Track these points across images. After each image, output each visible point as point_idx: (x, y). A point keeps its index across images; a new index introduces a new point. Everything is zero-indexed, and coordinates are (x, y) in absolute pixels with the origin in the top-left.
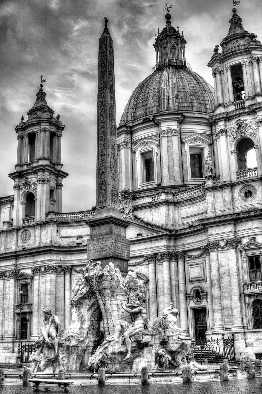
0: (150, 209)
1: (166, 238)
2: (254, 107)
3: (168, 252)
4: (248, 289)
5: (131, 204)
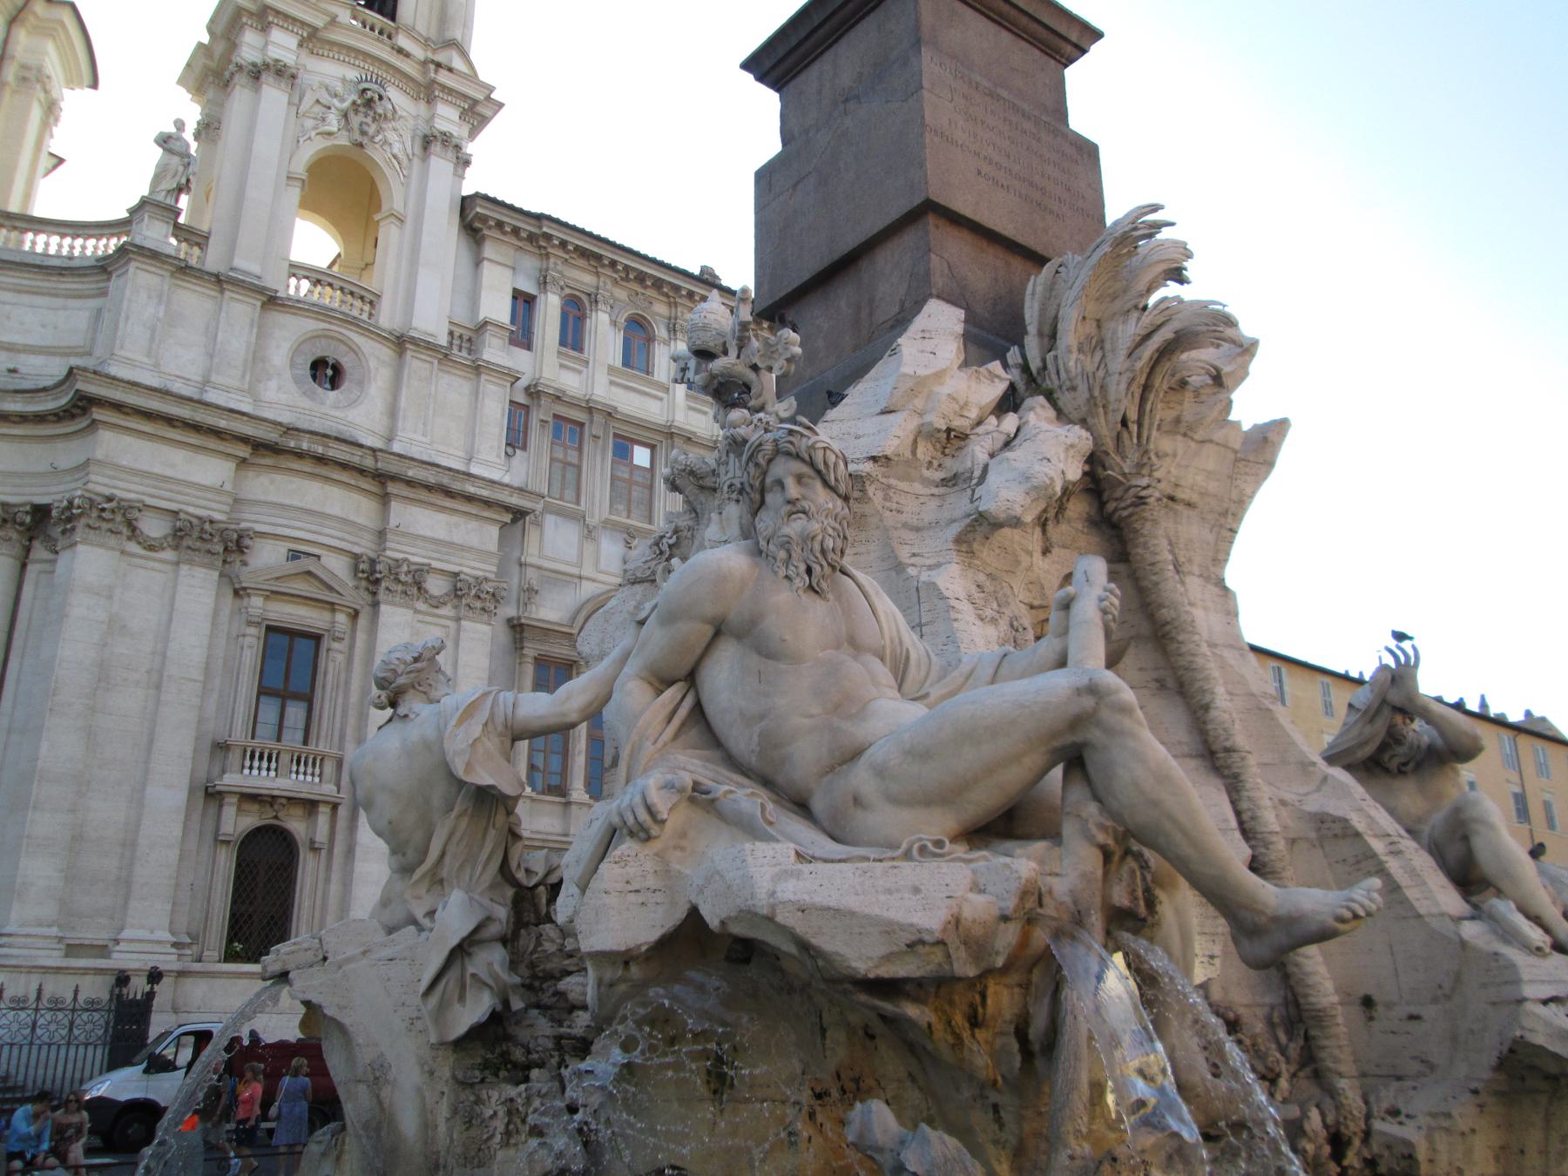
2: (443, 77)
4: (246, 771)
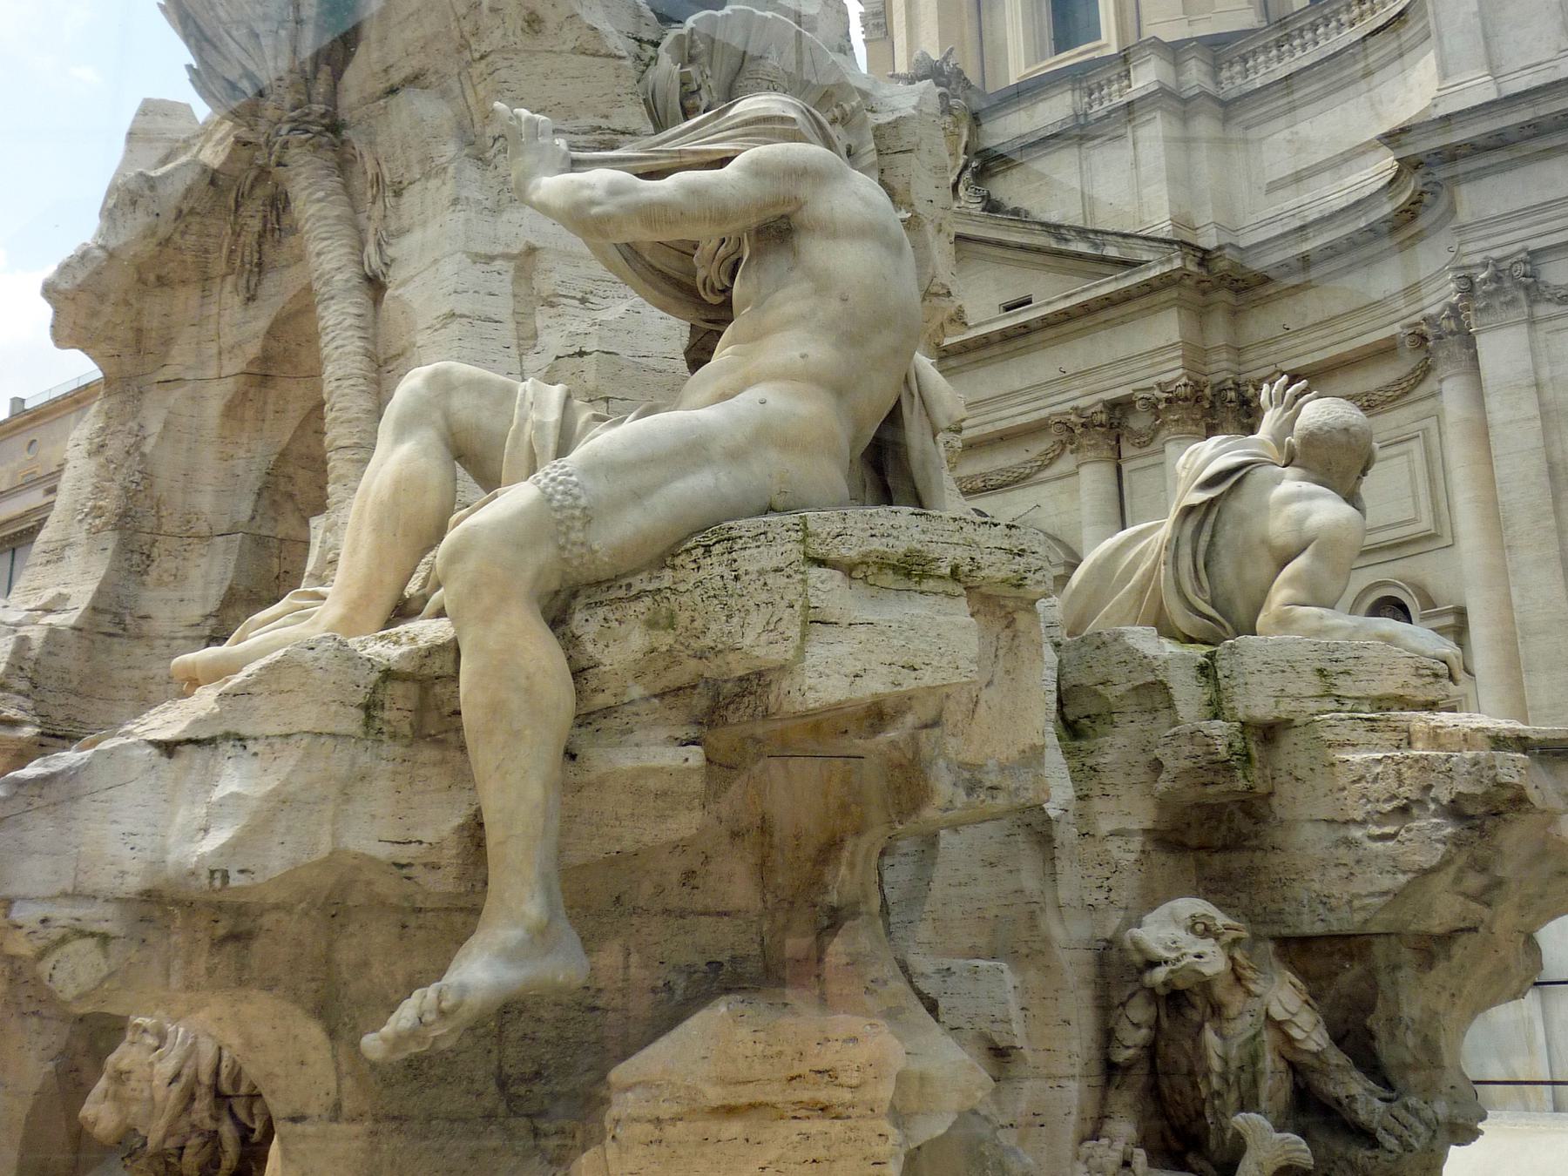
0: (1075, 150)
1: (1180, 304)
3: (1197, 382)
5: (965, 139)
